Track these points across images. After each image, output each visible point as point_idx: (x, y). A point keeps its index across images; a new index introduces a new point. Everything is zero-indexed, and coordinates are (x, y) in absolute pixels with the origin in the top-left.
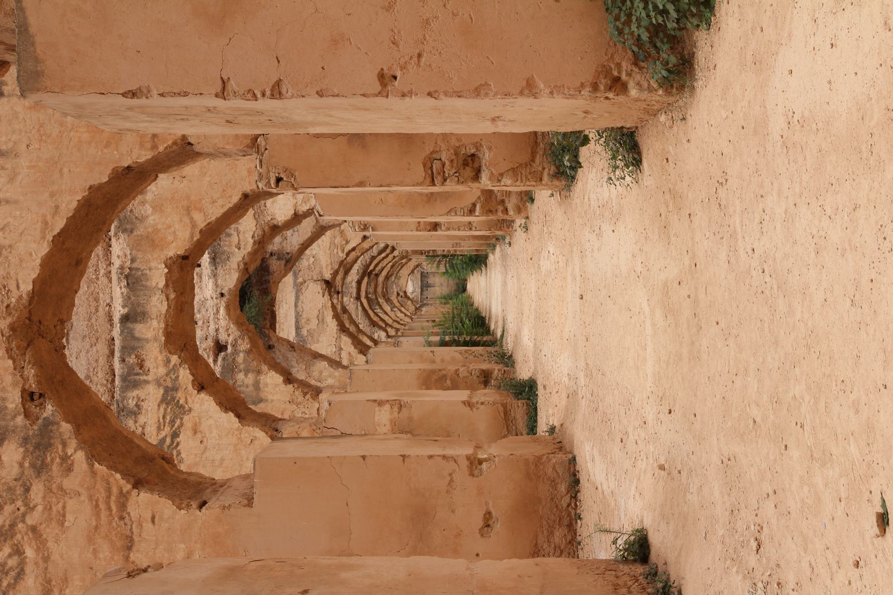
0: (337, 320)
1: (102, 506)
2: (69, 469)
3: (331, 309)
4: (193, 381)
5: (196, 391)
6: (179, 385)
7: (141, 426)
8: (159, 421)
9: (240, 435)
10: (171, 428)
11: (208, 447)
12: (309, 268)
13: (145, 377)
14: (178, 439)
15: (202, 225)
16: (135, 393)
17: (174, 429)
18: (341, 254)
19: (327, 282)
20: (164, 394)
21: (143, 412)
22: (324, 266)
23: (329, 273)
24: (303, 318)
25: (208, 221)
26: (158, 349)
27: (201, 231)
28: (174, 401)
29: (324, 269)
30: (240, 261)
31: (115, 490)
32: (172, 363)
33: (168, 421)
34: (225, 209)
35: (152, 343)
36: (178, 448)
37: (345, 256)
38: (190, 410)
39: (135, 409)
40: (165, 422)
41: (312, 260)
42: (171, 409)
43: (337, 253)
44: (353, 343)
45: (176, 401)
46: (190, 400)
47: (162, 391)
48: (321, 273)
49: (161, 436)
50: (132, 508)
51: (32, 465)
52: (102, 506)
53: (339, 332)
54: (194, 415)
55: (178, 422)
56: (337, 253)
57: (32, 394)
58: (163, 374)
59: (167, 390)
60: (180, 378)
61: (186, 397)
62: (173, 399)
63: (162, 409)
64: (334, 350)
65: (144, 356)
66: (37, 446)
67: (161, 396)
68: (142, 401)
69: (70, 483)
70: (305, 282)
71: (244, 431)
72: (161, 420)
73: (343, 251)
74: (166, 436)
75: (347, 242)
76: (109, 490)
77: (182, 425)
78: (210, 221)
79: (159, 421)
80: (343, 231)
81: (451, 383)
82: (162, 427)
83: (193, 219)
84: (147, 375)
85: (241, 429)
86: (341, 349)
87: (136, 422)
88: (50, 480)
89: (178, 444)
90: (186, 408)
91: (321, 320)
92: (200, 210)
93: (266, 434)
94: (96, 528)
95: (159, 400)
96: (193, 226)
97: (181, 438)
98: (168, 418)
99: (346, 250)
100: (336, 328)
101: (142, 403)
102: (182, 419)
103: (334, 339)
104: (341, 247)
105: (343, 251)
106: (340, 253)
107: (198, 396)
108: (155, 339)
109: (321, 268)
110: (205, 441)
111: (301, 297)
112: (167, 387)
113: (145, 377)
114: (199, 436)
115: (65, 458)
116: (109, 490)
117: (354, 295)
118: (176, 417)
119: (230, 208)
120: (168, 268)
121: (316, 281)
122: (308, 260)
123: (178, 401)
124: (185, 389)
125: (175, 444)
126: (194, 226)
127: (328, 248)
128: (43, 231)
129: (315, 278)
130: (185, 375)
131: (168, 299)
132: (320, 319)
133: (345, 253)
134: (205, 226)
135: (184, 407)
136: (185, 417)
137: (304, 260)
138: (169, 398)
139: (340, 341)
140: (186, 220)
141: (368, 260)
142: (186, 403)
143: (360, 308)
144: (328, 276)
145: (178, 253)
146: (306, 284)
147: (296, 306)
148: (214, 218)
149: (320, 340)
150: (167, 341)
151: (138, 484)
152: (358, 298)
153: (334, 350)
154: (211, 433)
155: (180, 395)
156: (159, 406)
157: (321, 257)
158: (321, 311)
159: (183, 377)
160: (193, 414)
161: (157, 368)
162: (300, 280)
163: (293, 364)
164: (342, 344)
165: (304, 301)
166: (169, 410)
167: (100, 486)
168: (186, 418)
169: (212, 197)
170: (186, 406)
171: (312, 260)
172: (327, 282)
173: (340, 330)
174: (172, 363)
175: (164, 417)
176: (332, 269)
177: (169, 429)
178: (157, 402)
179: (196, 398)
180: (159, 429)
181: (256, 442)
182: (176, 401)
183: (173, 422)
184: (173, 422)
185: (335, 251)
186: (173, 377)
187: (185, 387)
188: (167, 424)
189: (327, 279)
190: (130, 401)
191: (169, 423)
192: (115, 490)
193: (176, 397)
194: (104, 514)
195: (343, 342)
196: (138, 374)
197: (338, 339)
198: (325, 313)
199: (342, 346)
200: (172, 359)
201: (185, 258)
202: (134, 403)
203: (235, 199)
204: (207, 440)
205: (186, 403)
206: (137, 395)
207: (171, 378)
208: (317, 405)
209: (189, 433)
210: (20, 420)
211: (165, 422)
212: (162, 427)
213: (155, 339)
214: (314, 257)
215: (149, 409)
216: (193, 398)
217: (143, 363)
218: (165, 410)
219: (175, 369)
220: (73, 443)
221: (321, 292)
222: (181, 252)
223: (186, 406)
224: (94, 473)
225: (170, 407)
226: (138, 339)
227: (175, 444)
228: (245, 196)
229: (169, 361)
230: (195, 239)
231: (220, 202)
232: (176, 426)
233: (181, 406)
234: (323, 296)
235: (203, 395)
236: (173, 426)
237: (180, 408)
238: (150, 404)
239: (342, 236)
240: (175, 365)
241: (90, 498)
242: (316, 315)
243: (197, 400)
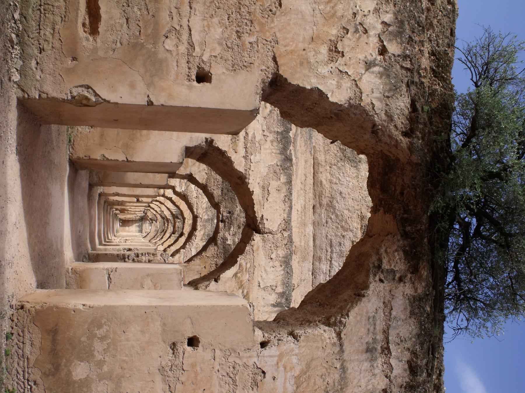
0: (249, 189)
3: (255, 202)
22: (261, 249)
23: (256, 242)
24: (283, 193)
43: (246, 264)
53: (247, 176)
56: (246, 264)
73: (240, 265)
75: (235, 275)
80: (239, 288)
86: (245, 157)
91: (265, 189)
100: (250, 181)
103: (252, 168)
104: (242, 270)
105: (240, 265)
106: (244, 264)
111: (285, 215)
117: (199, 220)
122: (278, 256)
132: (266, 192)
133: (238, 263)
137: (281, 255)
141: (187, 246)
143: (195, 210)
144: (257, 237)
146: (280, 230)
147: (291, 207)
149: (267, 169)
152: (195, 218)
153: (252, 157)
157: (264, 259)
162: (286, 234)
163: (379, 103)
164: (244, 163)
165: (282, 212)
171: (273, 256)
172: (259, 232)
173: (246, 178)
185: (248, 265)
189: (257, 235)
195: (243, 165)
198: (261, 198)
221: (265, 221)
234: (263, 216)
239: (241, 282)
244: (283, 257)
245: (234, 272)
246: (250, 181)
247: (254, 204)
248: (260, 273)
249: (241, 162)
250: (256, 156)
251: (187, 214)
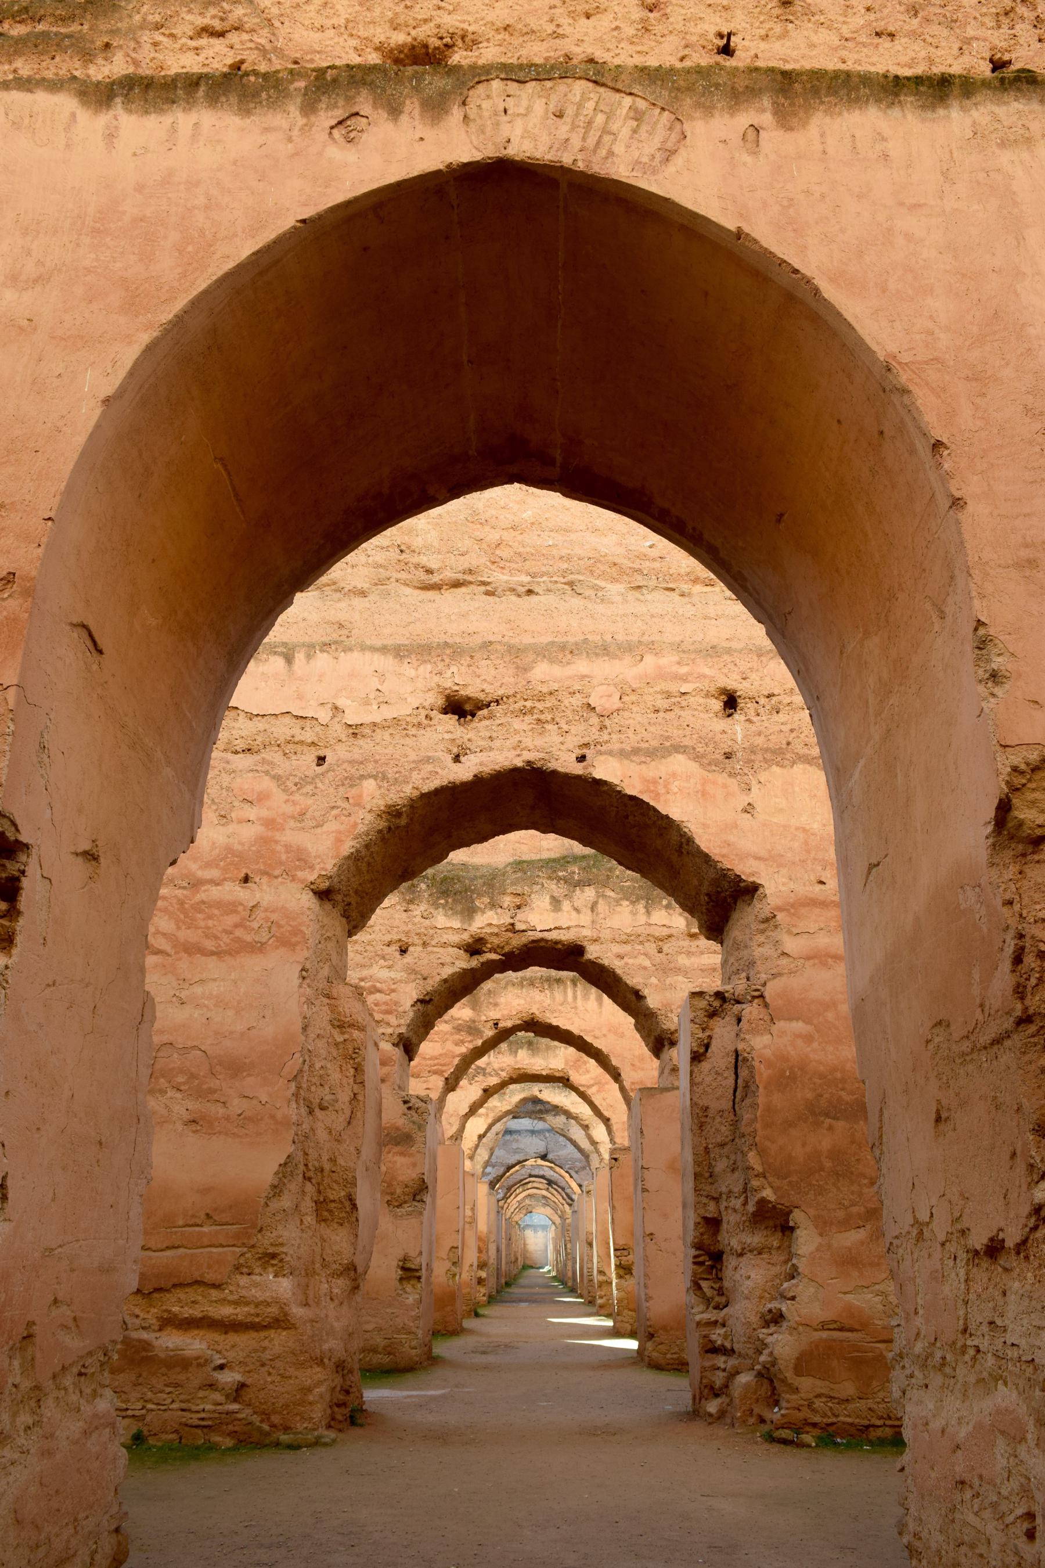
1: (436, 1061)
2: (456, 1045)
12: (557, 1142)
31: (444, 1068)
47: (483, 1066)
50: (434, 1077)
51: (460, 1025)
52: (436, 1061)
57: (496, 1024)
59: (484, 1069)
66: (470, 1027)
69: (450, 1046)
75: (577, 1172)
76: (444, 1065)
88: (452, 1034)
92: (598, 1091)
94: (425, 1058)
108: (516, 1062)
115: (463, 1042)
116: (444, 1065)
117: (533, 1173)
126: (589, 1087)
128: (585, 1030)
130: (494, 1081)
140: (592, 1082)
144: (550, 1156)
151: (447, 1079)
152: (531, 1176)
155: (480, 1078)
162: (547, 1135)
167: (447, 1060)
192: (444, 1068)
194: (429, 1062)
201: (568, 1080)
203: (606, 1114)
210: (484, 1018)
213: (516, 1062)
219: (497, 1074)
220: (471, 1046)
222: (571, 1078)
224: (454, 1057)
228: (608, 1120)
231: (604, 1104)
235: (480, 1092)
241: (441, 1055)
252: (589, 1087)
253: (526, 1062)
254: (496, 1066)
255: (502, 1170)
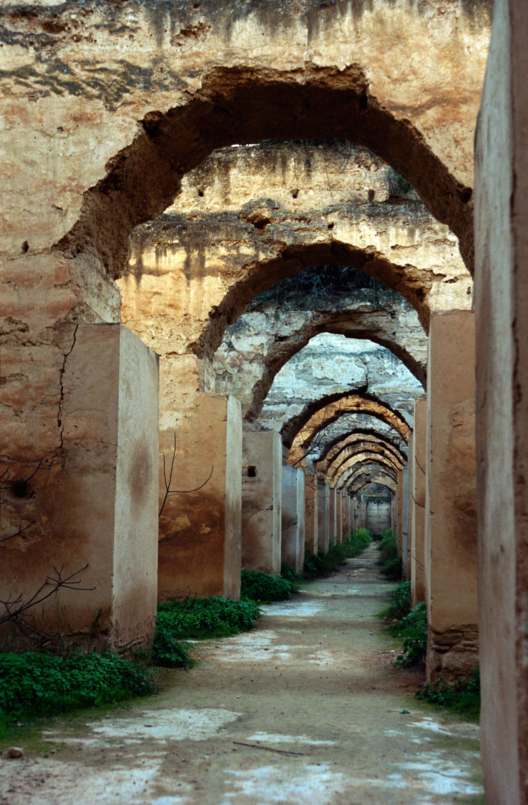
3: (334, 393)
4: (158, 113)
5: (142, 118)
6: (153, 92)
7: (91, 34)
8: (98, 62)
9: (70, 190)
10: (84, 82)
11: (52, 140)
12: (382, 369)
13: (167, 37)
14: (66, 93)
15: (418, 124)
16: (144, 25)
17: (84, 85)
18: (397, 404)
19: (365, 388)
20: (139, 68)
21: (113, 38)
22: (383, 385)
23: (375, 391)
25: (424, 133)
26: (213, 58)
27: (408, 122)
28: (128, 84)
29: (379, 386)
30: (375, 248)
32: (189, 81)
33: (97, 75)
34: (445, 162)
35: (223, 48)
36: (53, 94)
37: (394, 409)
38: (113, 110)
39: (119, 25)
40: (94, 71)
41: (391, 372)
42: (115, 80)
43: (399, 401)
44: (295, 417)
45: (128, 87)
46: (129, 108)
47: (145, 65)
48: (376, 382)
49: (73, 66)
54: (104, 116)
55: (95, 92)
56: (399, 401)
58: (172, 66)
59: (145, 73)
60: (165, 93)
61: (133, 103)
62: (131, 83)
63: (115, 66)
64: (289, 396)
65: (202, 36)
67: (137, 64)
68: (131, 36)
70: (365, 364)
71: (75, 195)
72: (98, 66)
73: (399, 407)
74: (73, 74)
75: (410, 412)
77: (90, 97)
78: (425, 136)
79: (98, 62)
81: (205, 534)
82: (87, 67)
83: (429, 108)
84: (172, 41)
85: (78, 192)
86: (289, 404)
87: (97, 27)
89: (59, 92)
90: (115, 104)
91: (321, 382)
92: (440, 122)
93: (70, 232)
95: (131, 61)
96: (416, 109)
97: (69, 97)
98: (102, 76)
99: (401, 411)
101: (126, 36)
102: (99, 97)
103: (300, 396)
104: (405, 405)
107: (135, 122)
108: (230, 54)
109: (382, 382)
110: (62, 135)
112: (151, 74)
113: (167, 37)
114: (71, 124)
117: (359, 426)
118: (102, 88)
119: (446, 169)
120: (345, 70)
121: (367, 376)
123: (127, 91)
124: (147, 102)
125: (59, 88)
126: (418, 111)
127: (404, 390)
129: (370, 375)
131: (294, 72)
132: (324, 381)
133: (398, 409)
134: (415, 129)
135: (116, 100)
136: (102, 103)
137: (390, 363)
138: (133, 77)
139: (298, 403)
140: (425, 98)
142: (123, 104)
143: (345, 432)
145: (370, 86)
146: (364, 366)
148: (429, 142)
149: (300, 381)
150: (225, 71)
153: (289, 396)
154: (75, 144)
155: (138, 93)
156: (122, 62)
158: (333, 382)
159: (167, 98)
160: (106, 113)
161: (182, 58)
162: (368, 358)
164: (294, 405)
166: (115, 77)
168: (100, 104)
169: (464, 139)
170: (119, 104)
172: (365, 388)
173: (310, 403)
174: (189, 81)
175: (103, 70)
176: (380, 394)
177: (84, 78)
178: (128, 59)
179: (131, 120)
180: (84, 63)
181: (57, 217)
182: (128, 87)
183: (96, 84)
184: (96, 84)
185: (401, 398)
186: (167, 83)
187: (149, 100)
188: (91, 74)
189: (368, 390)
190: (131, 17)
191: (93, 78)
193: (135, 87)
196: (173, 29)
197: (300, 401)
198: (330, 387)
199: (292, 406)
200: (196, 79)
202: (129, 24)
204: (64, 138)
205: (123, 104)
206: (140, 28)
207: (165, 79)
208: (180, 352)
209: (76, 109)
211: (94, 71)
212: (87, 67)
213: (230, 54)
214: (393, 374)
215: (118, 47)
216: (132, 114)
217: (193, 36)
218: (115, 72)
221: (354, 382)
223: (119, 104)
225: (118, 78)
226: (229, 27)
227: (59, 88)
229: (192, 76)
230: (394, 113)
232: (89, 89)
233: (120, 96)
234: (349, 384)
235: (135, 130)
236: (88, 84)
237: (117, 93)
238: (125, 48)
240: (186, 85)
242: (327, 376)
243: (128, 120)
244: (392, 361)
245: (407, 413)
246: (313, 398)
247: (337, 394)
248: (408, 386)
249: (293, 408)
250: (287, 393)
251: (353, 438)
252: (418, 111)
253: (255, 53)
254: (177, 65)
255: (300, 409)
